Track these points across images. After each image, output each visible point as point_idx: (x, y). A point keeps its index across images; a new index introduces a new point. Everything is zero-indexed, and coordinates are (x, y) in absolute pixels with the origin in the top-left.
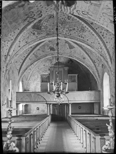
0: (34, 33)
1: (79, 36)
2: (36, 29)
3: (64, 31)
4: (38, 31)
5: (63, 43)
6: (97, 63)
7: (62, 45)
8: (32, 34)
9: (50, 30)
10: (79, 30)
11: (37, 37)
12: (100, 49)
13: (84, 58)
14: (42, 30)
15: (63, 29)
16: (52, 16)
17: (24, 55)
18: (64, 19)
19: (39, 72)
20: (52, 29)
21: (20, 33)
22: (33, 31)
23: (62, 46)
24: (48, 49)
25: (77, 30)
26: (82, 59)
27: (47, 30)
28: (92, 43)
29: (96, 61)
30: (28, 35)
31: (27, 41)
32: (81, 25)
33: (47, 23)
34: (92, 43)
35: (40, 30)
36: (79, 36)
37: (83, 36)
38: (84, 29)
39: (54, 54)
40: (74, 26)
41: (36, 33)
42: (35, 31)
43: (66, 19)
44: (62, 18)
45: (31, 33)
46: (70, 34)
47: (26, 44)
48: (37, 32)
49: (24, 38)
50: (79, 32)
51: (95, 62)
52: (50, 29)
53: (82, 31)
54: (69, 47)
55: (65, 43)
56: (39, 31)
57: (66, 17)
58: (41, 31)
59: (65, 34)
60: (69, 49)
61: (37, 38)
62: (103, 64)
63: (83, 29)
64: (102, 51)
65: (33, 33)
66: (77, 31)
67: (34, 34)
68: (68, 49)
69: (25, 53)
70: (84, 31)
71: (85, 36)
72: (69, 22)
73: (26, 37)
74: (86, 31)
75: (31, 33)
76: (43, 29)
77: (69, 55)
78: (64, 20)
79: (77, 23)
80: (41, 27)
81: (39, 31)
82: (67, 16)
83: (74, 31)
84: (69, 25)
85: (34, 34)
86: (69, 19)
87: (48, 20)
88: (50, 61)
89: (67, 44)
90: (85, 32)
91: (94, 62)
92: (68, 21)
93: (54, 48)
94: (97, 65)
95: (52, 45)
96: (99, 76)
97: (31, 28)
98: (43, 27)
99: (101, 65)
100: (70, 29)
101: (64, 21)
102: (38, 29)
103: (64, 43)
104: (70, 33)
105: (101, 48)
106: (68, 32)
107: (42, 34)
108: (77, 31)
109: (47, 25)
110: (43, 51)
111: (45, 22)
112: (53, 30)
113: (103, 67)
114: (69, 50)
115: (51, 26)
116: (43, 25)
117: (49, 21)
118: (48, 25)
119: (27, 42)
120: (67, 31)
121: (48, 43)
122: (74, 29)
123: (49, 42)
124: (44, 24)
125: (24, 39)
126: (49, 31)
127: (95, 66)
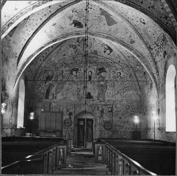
5: (97, 15)
6: (156, 50)
7: (95, 18)
12: (165, 19)
13: (133, 42)
17: (29, 33)
19: (55, 66)
23: (95, 20)
24: (71, 24)
26: (129, 44)
28: (149, 8)
29: (152, 47)
34: (149, 8)
39: (81, 34)
51: (150, 48)
54: (106, 23)
55: (101, 14)
60: (106, 25)
62: (165, 52)
64: (167, 23)
68: (104, 24)
69: (31, 29)
77: (107, 35)
88: (74, 49)
89: (104, 17)
91: (150, 48)
93: (82, 22)
94: (155, 52)
95: (77, 17)
96: (158, 72)
99: (162, 54)
103: (99, 15)
105: (166, 17)
110: (62, 27)
113: (166, 57)
114: (107, 28)
121: (72, 13)
123: (73, 12)
127: (152, 55)
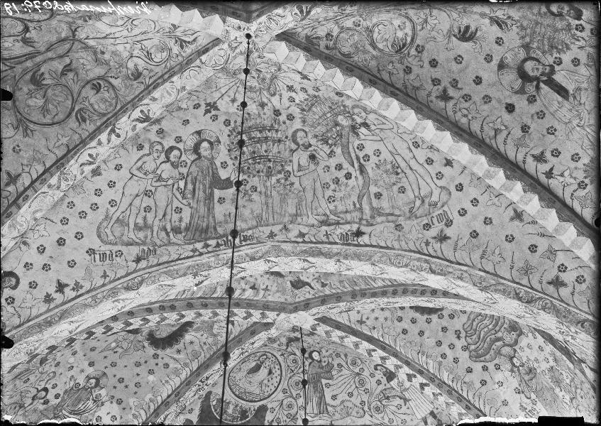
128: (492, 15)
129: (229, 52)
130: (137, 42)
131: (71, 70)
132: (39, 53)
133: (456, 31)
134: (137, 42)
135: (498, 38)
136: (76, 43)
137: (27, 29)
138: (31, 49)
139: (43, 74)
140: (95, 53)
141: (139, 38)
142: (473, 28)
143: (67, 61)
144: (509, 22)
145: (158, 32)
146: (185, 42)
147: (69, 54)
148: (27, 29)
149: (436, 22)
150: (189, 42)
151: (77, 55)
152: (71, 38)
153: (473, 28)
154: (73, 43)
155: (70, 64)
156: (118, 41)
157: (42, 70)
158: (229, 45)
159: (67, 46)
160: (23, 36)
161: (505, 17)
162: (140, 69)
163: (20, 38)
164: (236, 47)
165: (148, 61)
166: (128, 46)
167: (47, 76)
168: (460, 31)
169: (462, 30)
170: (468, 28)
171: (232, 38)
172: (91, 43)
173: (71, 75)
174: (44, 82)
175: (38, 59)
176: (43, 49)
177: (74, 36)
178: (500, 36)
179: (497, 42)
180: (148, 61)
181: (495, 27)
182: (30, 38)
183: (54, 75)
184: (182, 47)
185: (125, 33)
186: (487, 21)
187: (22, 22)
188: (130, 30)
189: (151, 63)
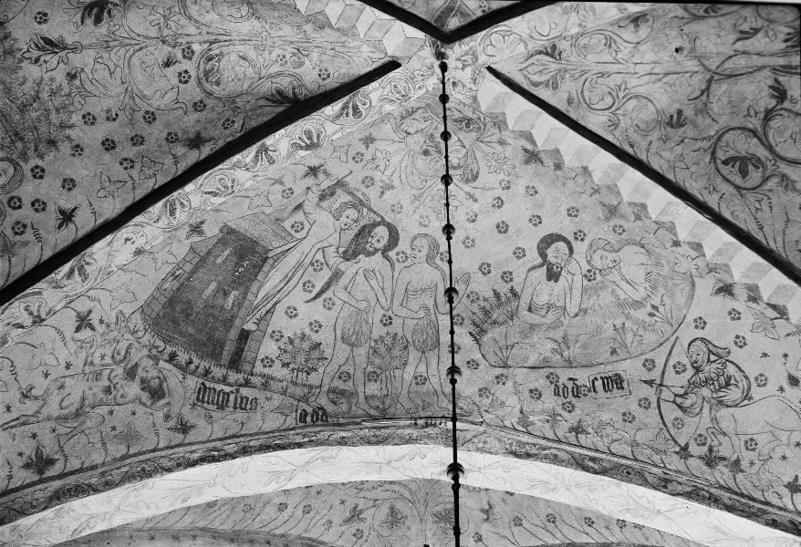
0: (162, 380)
1: (684, 452)
2: (194, 345)
3: (502, 392)
4: (207, 372)
8: (133, 389)
9: (349, 386)
10: (666, 395)
11: (184, 428)
14: (259, 368)
15: (486, 374)
16: (382, 232)
18: (507, 277)
20: (372, 377)
21: (59, 499)
22: (156, 360)
25: (650, 392)
27: (314, 379)
30: (77, 389)
31: (49, 449)
32: (688, 333)
33: (316, 311)
35: (235, 363)
36: (685, 449)
37: (724, 451)
38: (731, 370)
40: (614, 352)
41: (181, 387)
42: (172, 357)
43: (519, 269)
44: (485, 269)
45: (131, 374)
46: (578, 429)
47: (30, 476)
48: (193, 382)
49: (30, 407)
50: (671, 413)
52: (346, 376)
53: (706, 392)
56: (218, 372)
57: (520, 253)
58: (247, 384)
59: (512, 420)
61: (179, 437)
63: (710, 370)
65: (145, 385)
66: (644, 403)
67: (157, 393)
70: (734, 394)
71: (751, 444)
72: (549, 307)
73: (53, 409)
74: (756, 392)
75: (119, 371)
76: (268, 362)
78: (504, 289)
79: (641, 314)
80: (244, 336)
81: (224, 380)
82: (530, 243)
83: (618, 402)
84: (559, 334)
85: (157, 393)
86: (553, 276)
87: (337, 275)
90: (747, 397)
92: (545, 292)
97: (137, 320)
98: (269, 348)
100: (564, 375)
101: (497, 294)
102: (215, 355)
104: (572, 419)
106: (550, 401)
107: (242, 404)
108: (644, 403)
109: (316, 338)
111: (297, 298)
112: (373, 388)
115: (362, 352)
116: (279, 321)
117: (337, 292)
118: (325, 337)
119: (51, 462)
120: (536, 394)
122: (615, 382)
124: (292, 313)
125: (23, 421)
126: (332, 391)
128: (63, 53)
129: (480, 49)
130: (620, 63)
131: (741, 32)
132: (774, 69)
133: (114, 12)
134: (620, 63)
135: (45, 21)
136: (713, 67)
137: (769, 115)
138: (780, 79)
139: (786, 41)
140: (693, 49)
141: (616, 68)
142: (89, 21)
143: (739, 45)
144: (35, 53)
145: (583, 73)
146: (547, 54)
147: (733, 53)
148: (769, 115)
149: (152, 18)
150: (541, 52)
151: (723, 49)
152: (716, 77)
153: (89, 21)
154: (718, 67)
155: (739, 40)
156: (647, 68)
157: (784, 45)
158: (477, 60)
159: (729, 65)
160: (779, 107)
161: (42, 58)
162: (631, 27)
163: (786, 104)
164: (466, 54)
165: (615, 37)
166: (636, 60)
167: (783, 37)
168: (109, 13)
169: (106, 14)
170: (98, 20)
171: (469, 70)
172: (691, 65)
173: (746, 27)
174: (792, 31)
175: (782, 61)
176: (766, 72)
177: (710, 81)
178: (44, 26)
179: (46, 15)
180: (615, 37)
181: (54, 36)
182: (773, 96)
183: (771, 33)
184: (554, 47)
185: (633, 82)
186: (69, 40)
187: (766, 136)
188: (623, 87)
189: (611, 34)
